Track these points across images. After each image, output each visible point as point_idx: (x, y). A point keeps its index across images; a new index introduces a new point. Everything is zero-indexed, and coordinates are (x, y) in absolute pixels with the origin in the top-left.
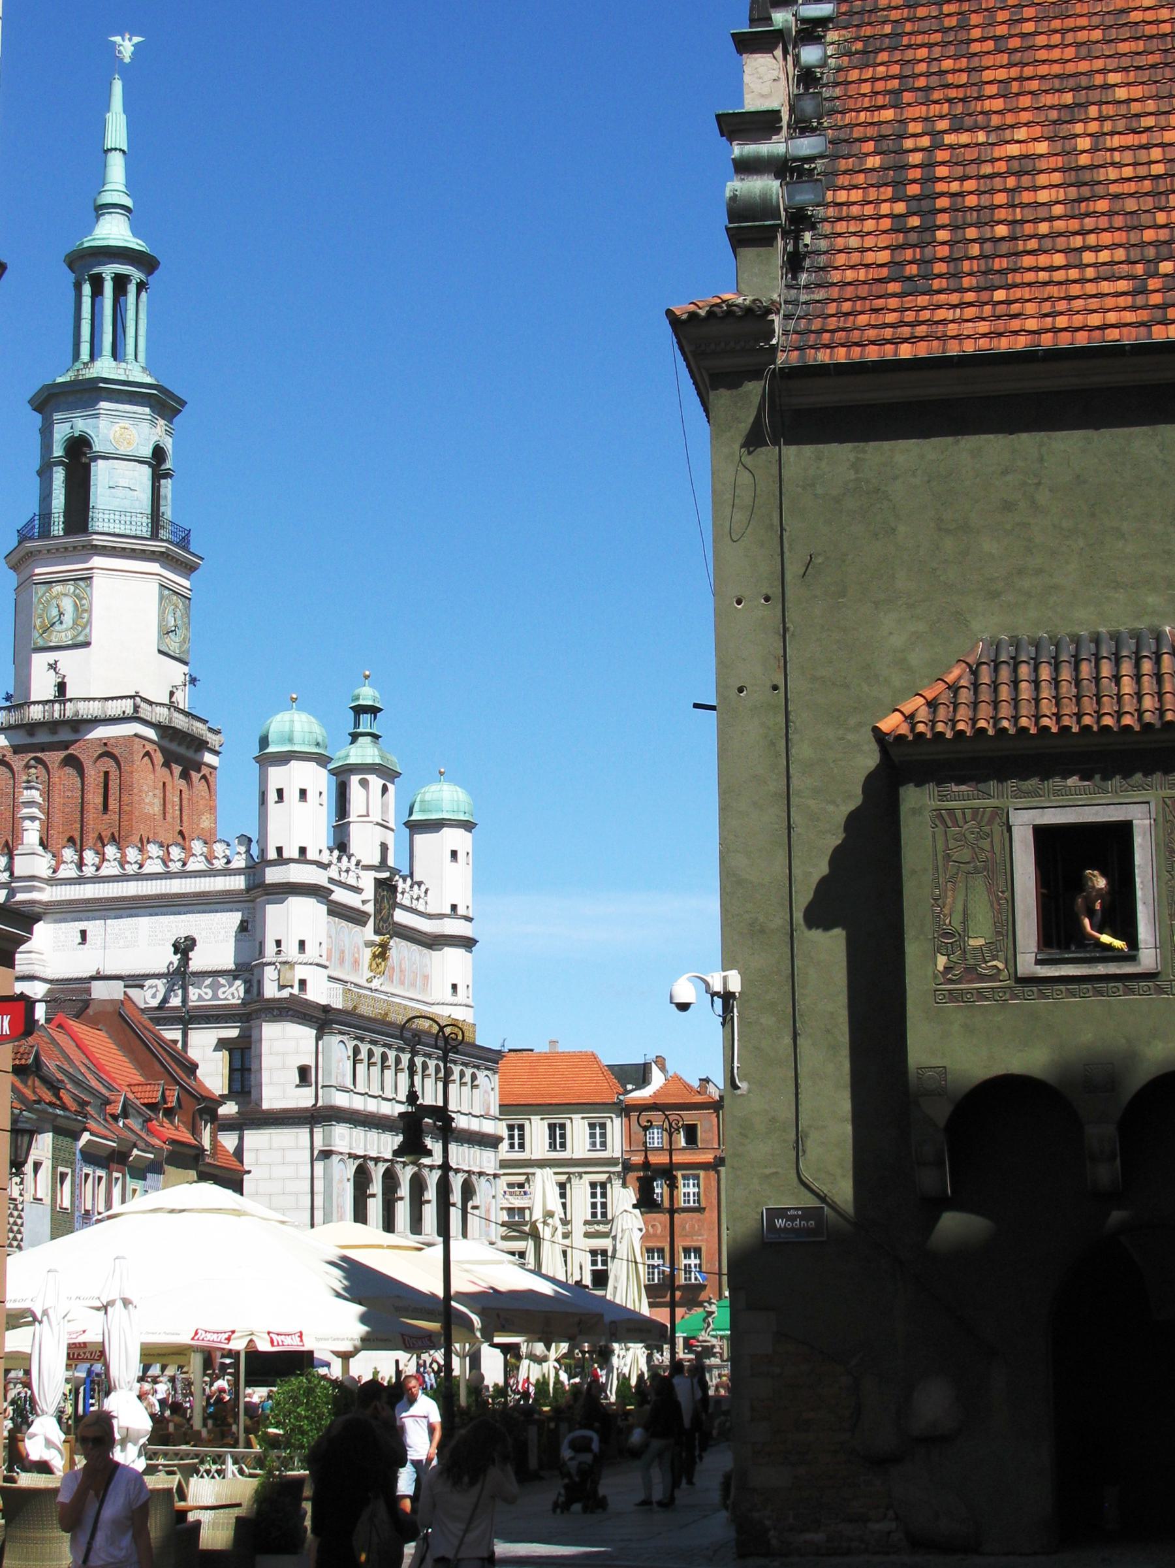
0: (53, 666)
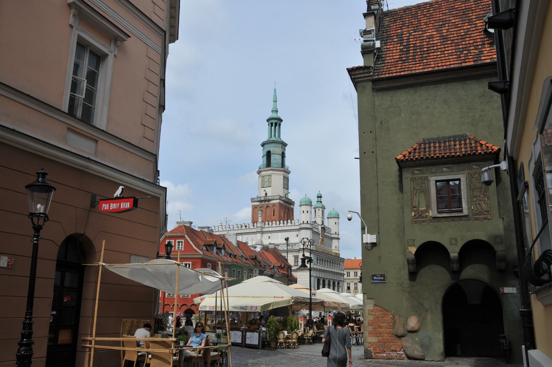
0: (265, 191)
